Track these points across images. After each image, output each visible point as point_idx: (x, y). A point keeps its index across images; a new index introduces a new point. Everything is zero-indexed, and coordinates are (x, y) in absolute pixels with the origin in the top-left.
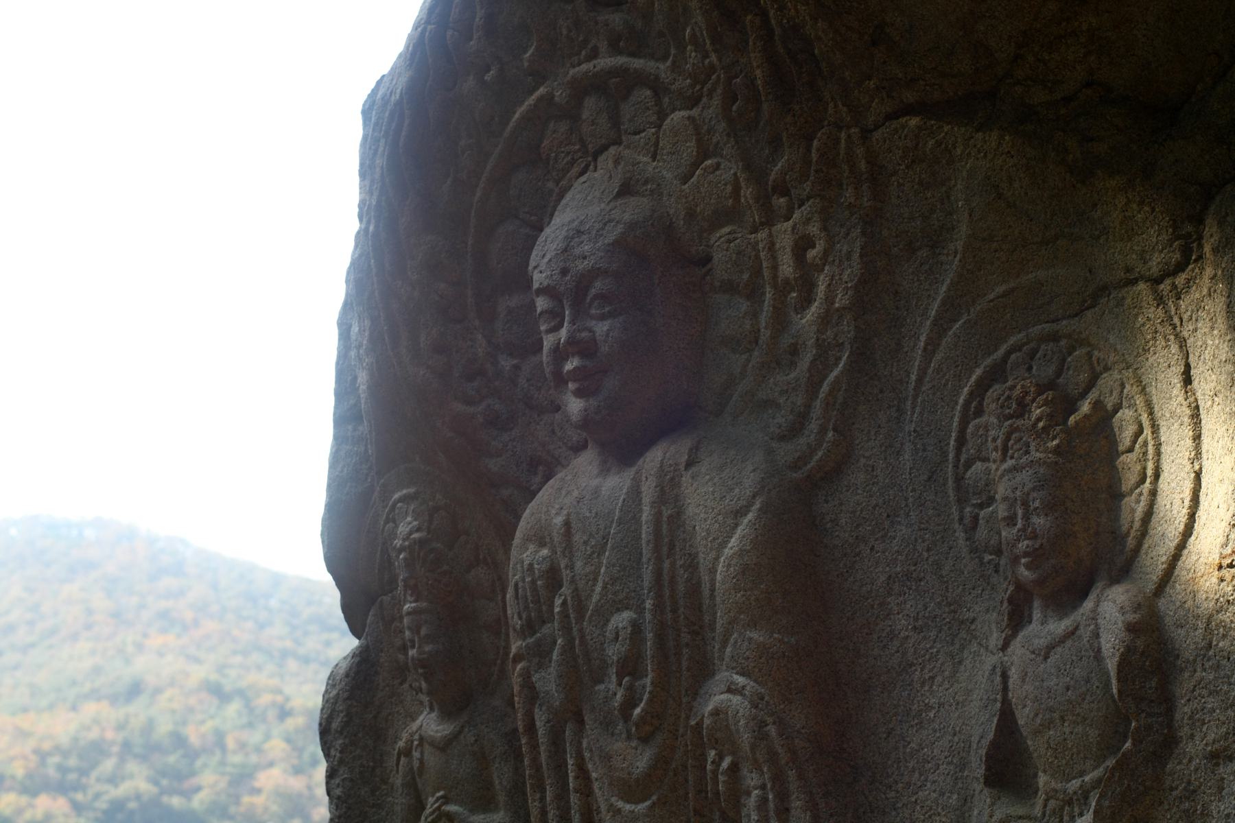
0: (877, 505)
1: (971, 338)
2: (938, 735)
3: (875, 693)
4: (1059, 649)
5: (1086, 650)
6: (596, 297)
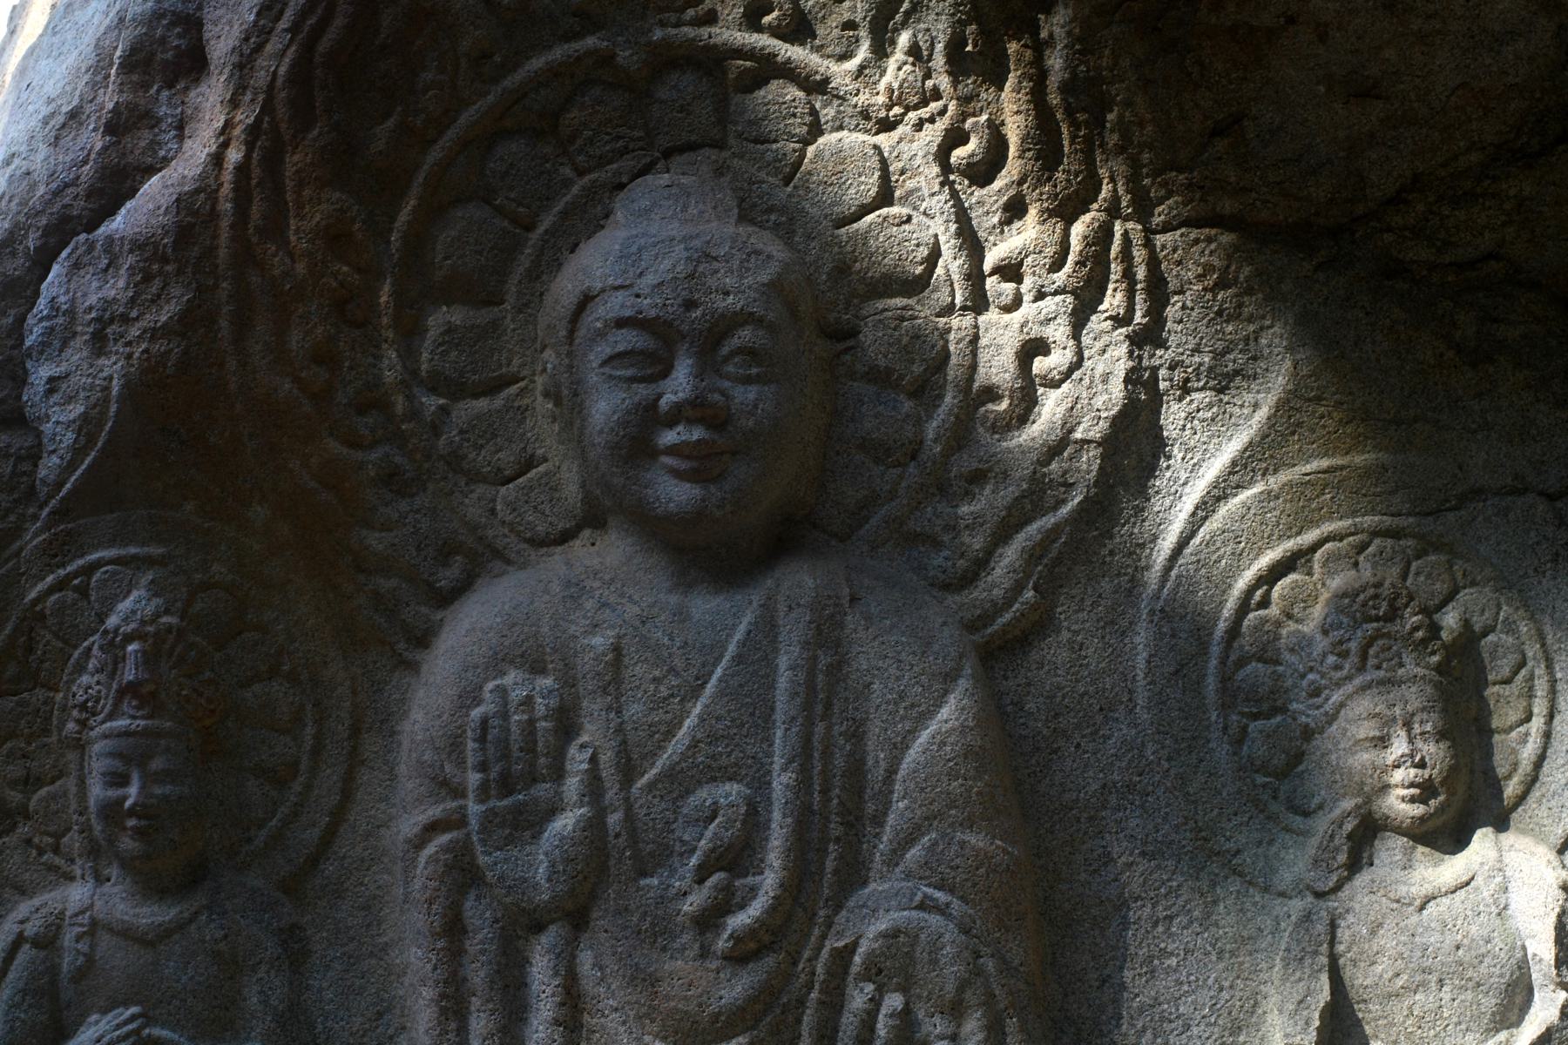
0: (1086, 693)
1: (1266, 513)
2: (1186, 988)
3: (1082, 929)
4: (1445, 901)
5: (1487, 906)
6: (740, 351)
